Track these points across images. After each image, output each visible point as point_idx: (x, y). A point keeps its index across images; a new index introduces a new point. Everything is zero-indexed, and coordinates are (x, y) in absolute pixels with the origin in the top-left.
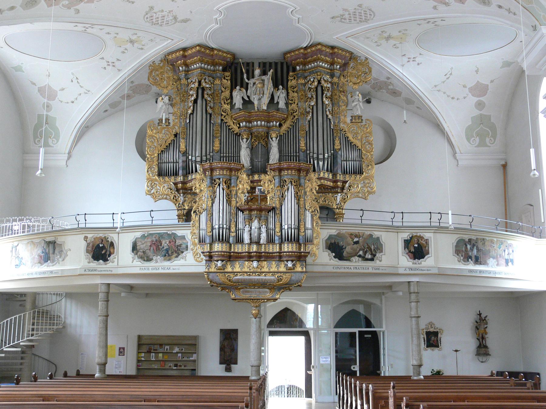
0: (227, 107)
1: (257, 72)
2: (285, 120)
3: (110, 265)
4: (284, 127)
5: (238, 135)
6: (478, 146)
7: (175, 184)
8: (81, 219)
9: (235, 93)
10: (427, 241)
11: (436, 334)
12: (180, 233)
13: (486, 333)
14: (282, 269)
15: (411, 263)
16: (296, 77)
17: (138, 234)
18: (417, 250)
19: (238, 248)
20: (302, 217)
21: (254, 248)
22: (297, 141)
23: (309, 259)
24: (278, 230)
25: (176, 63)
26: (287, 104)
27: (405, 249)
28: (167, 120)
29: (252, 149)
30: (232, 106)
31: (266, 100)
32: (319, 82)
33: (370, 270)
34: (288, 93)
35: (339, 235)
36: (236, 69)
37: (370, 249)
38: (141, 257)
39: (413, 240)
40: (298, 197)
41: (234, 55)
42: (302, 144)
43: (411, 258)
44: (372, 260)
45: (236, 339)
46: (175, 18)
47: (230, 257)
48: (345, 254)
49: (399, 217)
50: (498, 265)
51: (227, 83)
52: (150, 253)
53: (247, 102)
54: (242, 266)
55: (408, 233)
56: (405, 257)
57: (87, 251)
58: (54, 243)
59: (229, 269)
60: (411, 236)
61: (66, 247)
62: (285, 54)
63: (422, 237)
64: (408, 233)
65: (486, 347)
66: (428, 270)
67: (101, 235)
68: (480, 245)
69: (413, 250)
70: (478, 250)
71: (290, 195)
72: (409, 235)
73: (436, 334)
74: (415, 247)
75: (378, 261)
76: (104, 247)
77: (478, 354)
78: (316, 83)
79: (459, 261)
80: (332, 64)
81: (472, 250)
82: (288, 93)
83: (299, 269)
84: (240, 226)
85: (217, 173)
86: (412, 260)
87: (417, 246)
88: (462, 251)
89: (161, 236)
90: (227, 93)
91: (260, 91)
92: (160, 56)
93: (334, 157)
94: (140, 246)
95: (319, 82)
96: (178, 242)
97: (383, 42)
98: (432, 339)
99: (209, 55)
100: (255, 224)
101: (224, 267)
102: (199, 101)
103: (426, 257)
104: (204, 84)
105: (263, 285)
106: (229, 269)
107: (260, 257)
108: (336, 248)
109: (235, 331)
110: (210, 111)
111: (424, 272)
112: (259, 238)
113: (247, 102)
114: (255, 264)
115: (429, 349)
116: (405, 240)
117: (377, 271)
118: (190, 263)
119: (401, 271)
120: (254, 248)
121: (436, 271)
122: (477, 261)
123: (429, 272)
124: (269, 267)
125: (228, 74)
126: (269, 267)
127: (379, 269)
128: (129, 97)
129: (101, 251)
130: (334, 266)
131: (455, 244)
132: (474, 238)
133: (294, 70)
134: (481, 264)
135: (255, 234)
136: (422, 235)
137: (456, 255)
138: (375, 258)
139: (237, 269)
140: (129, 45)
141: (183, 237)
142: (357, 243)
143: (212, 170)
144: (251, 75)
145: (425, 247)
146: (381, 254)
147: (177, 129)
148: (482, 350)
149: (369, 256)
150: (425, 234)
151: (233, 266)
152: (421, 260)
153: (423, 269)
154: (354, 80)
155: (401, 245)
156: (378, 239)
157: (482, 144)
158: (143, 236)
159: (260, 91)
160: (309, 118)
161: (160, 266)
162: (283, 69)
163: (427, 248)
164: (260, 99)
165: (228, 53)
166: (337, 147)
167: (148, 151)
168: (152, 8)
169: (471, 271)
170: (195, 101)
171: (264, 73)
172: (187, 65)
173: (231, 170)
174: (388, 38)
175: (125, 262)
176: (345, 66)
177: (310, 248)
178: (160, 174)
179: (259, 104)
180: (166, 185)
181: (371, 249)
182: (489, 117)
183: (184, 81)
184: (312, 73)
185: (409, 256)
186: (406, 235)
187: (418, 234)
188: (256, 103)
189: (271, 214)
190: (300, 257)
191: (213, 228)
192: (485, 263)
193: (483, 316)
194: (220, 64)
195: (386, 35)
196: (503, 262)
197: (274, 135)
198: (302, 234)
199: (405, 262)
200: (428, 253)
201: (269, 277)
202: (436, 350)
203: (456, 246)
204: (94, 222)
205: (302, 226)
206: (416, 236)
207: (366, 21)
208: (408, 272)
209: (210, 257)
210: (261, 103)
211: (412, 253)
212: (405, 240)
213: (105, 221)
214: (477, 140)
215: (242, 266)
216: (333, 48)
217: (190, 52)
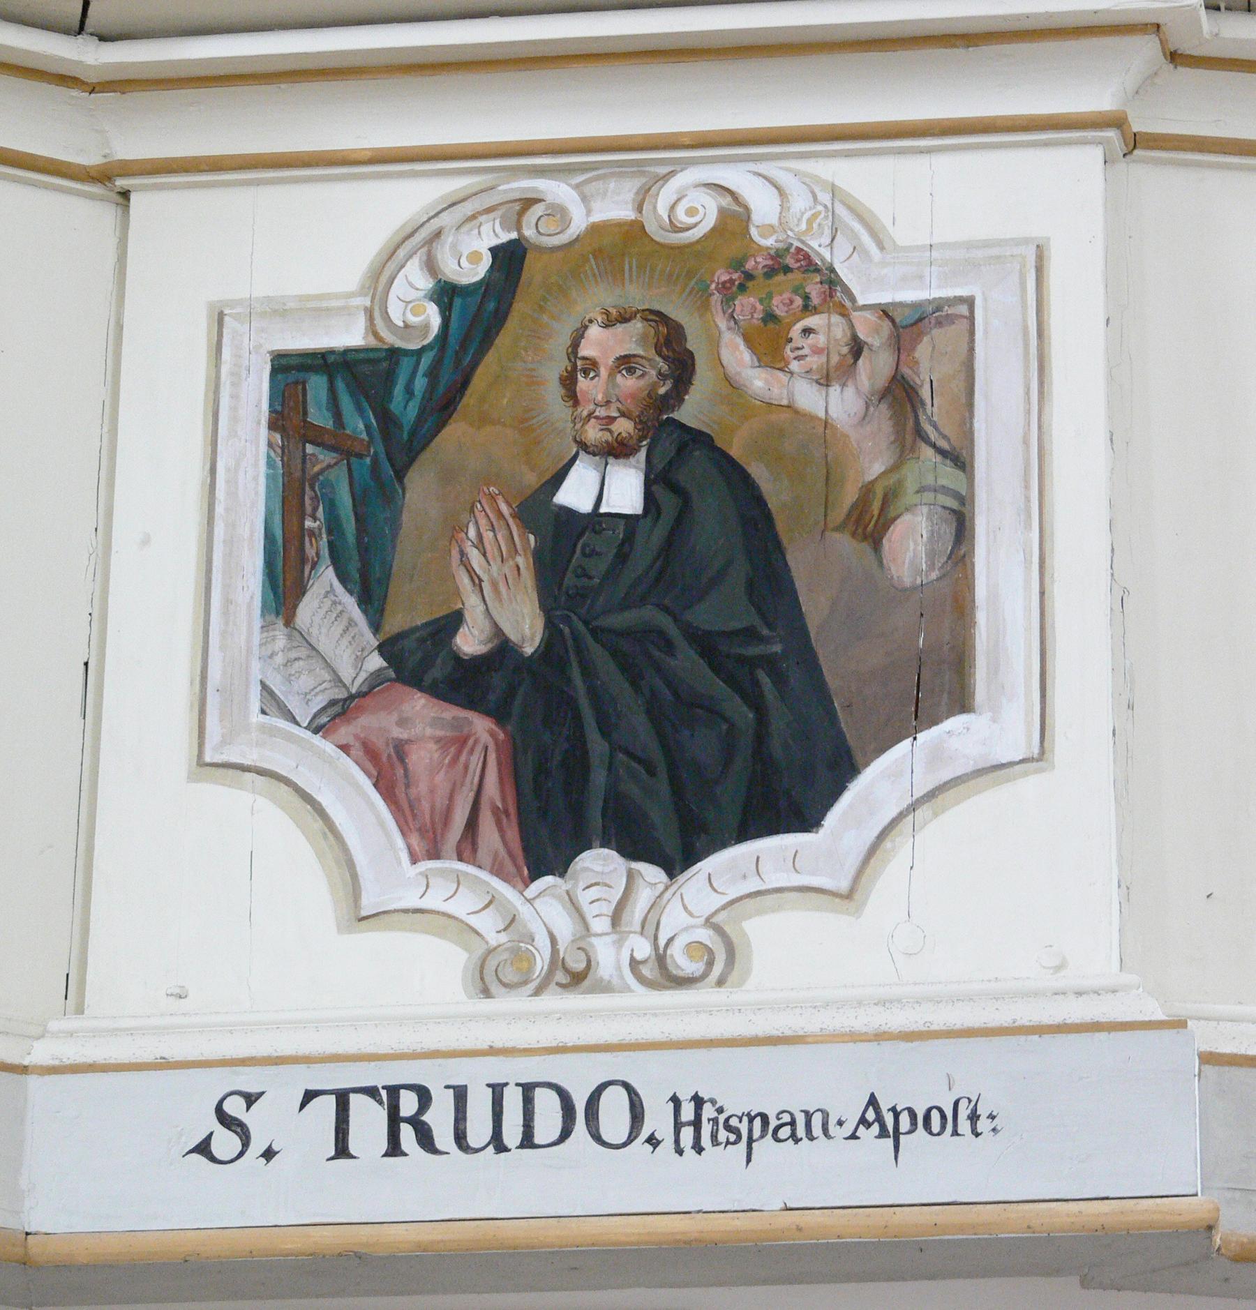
10: (916, 373)
27: (284, 590)
39: (524, 362)
60: (469, 260)
66: (884, 1122)
69: (502, 609)
72: (422, 238)
74: (564, 542)
86: (469, 893)
87: (625, 491)
116: (291, 371)
123: (935, 1175)
136: (775, 202)
145: (870, 522)
150: (862, 176)
152: (730, 867)
155: (189, 481)
185: (387, 771)
186: (337, 255)
187: (687, 203)
200: (938, 681)
206: (620, 247)
212: (291, 371)
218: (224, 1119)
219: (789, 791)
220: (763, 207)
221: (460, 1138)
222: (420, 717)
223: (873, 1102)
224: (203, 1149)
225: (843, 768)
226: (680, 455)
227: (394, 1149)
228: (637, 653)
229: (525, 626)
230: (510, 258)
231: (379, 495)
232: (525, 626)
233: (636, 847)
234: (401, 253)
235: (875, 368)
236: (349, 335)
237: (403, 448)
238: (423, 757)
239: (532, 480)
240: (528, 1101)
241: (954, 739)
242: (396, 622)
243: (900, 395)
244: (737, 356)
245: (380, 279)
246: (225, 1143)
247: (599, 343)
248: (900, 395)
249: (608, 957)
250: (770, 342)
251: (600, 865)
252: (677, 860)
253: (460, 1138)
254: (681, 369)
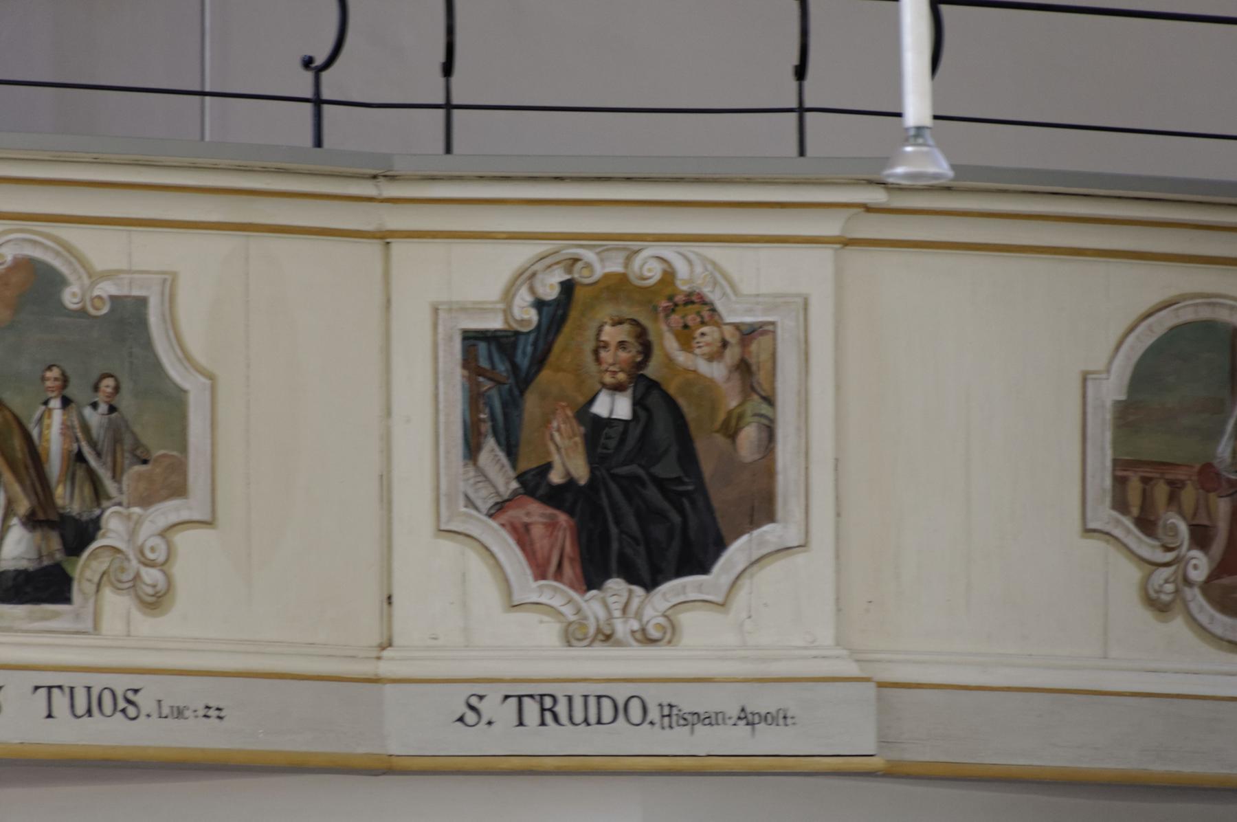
15: (547, 632)
27: (472, 450)
43: (540, 573)
55: (524, 253)
56: (476, 565)
60: (549, 288)
63: (695, 300)
64: (524, 253)
66: (747, 718)
69: (570, 463)
72: (527, 276)
74: (596, 428)
75: (115, 604)
79: (1158, 606)
86: (557, 595)
88: (1208, 476)
103: (737, 553)
111: (705, 741)
116: (471, 339)
117: (107, 733)
121: (852, 732)
123: (769, 740)
127: (127, 705)
131: (1113, 389)
136: (689, 270)
137: (1125, 528)
138: (86, 569)
145: (731, 430)
146: (167, 512)
153: (689, 700)
156: (127, 319)
163: (749, 435)
181: (36, 457)
185: (522, 535)
186: (487, 277)
199: (479, 612)
200: (761, 507)
203: (1128, 416)
206: (617, 287)
208: (501, 737)
211: (557, 497)
218: (472, 708)
219: (697, 555)
220: (682, 269)
221: (571, 718)
222: (535, 512)
223: (743, 710)
224: (461, 719)
225: (720, 545)
226: (646, 391)
227: (543, 723)
228: (630, 486)
229: (580, 470)
230: (568, 287)
231: (512, 404)
232: (580, 470)
233: (632, 577)
234: (518, 282)
235: (732, 354)
236: (495, 323)
237: (523, 381)
238: (538, 531)
239: (581, 400)
240: (599, 704)
241: (769, 534)
242: (524, 465)
243: (744, 368)
244: (671, 344)
245: (509, 295)
246: (471, 717)
247: (611, 334)
248: (744, 368)
249: (622, 628)
250: (686, 337)
251: (616, 586)
252: (650, 585)
253: (571, 718)
254: (646, 349)
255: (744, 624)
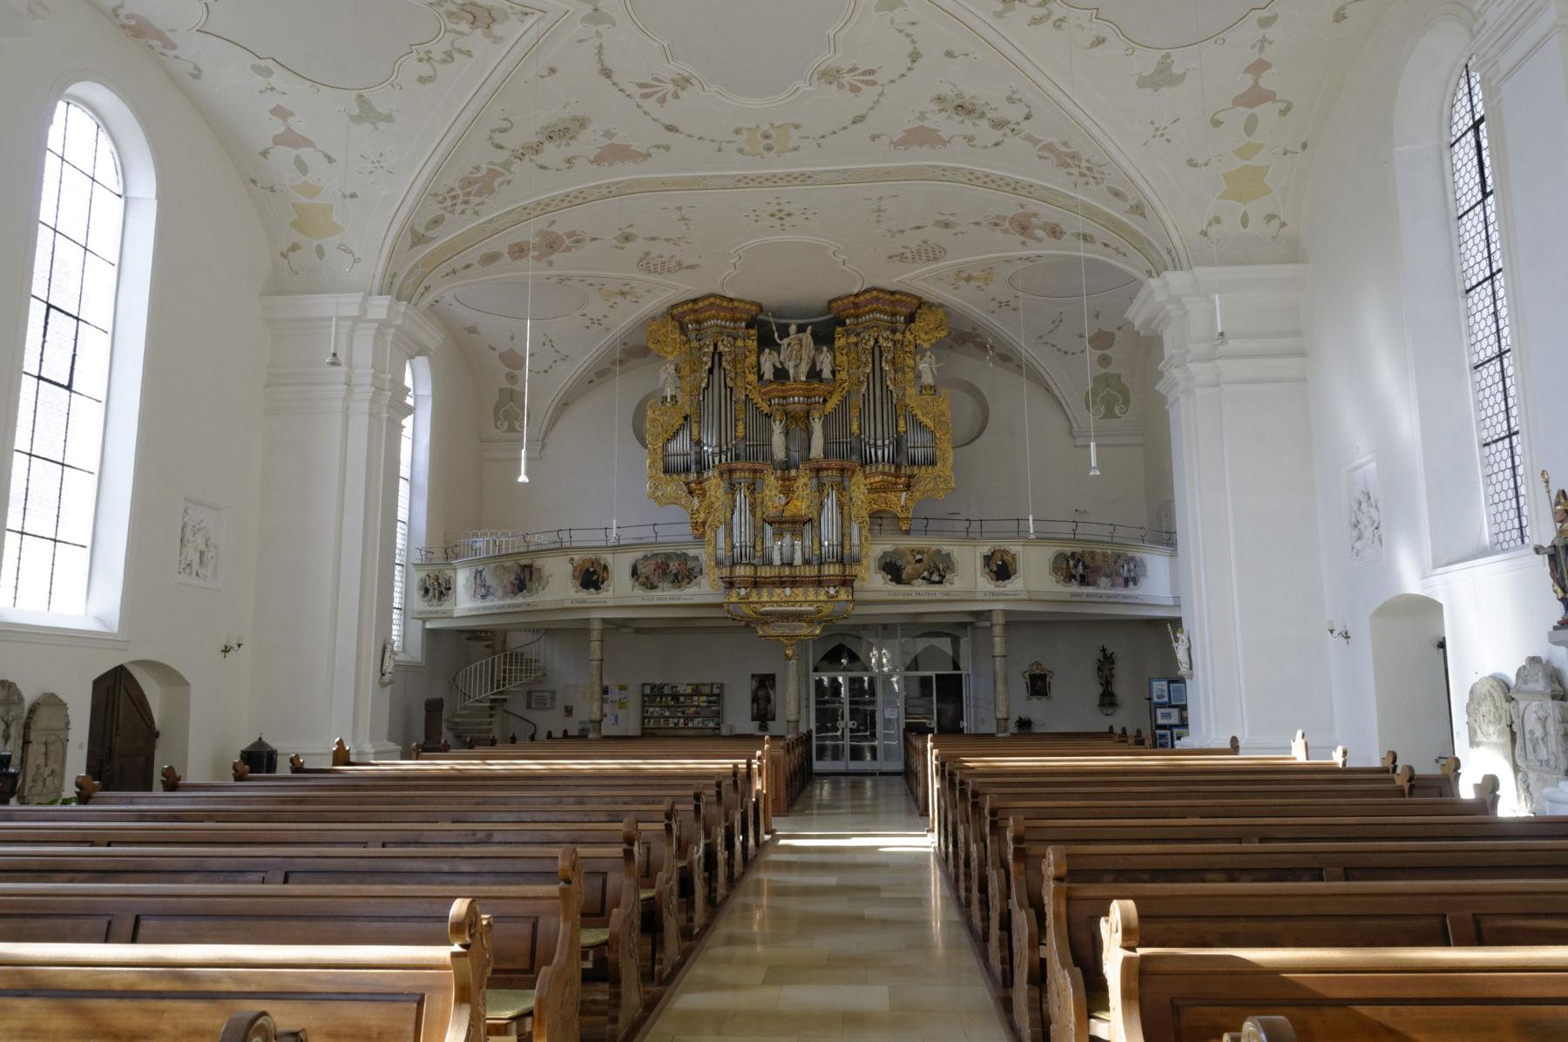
0: (752, 378)
1: (793, 329)
2: (831, 393)
3: (603, 594)
4: (830, 406)
5: (768, 416)
6: (1104, 417)
7: (687, 484)
8: (565, 535)
9: (762, 359)
10: (1014, 557)
11: (1043, 677)
12: (692, 552)
13: (1112, 676)
14: (823, 597)
16: (848, 334)
17: (639, 555)
18: (1002, 569)
19: (765, 572)
20: (846, 531)
21: (787, 571)
22: (846, 422)
23: (856, 584)
24: (816, 546)
25: (685, 318)
26: (833, 373)
28: (674, 397)
29: (787, 433)
30: (761, 377)
31: (804, 368)
32: (876, 341)
33: (938, 597)
34: (835, 358)
35: (896, 552)
36: (765, 328)
37: (938, 569)
38: (644, 584)
40: (841, 506)
41: (761, 309)
42: (855, 427)
44: (940, 582)
45: (773, 686)
46: (679, 264)
47: (756, 584)
48: (904, 576)
49: (975, 526)
50: (1113, 585)
51: (752, 344)
52: (654, 579)
53: (781, 374)
54: (771, 595)
57: (574, 577)
58: (530, 567)
59: (754, 598)
61: (546, 572)
62: (830, 302)
65: (1112, 695)
67: (591, 555)
68: (1087, 559)
70: (1085, 567)
71: (831, 503)
73: (1043, 677)
76: (595, 572)
77: (1102, 704)
78: (872, 342)
80: (894, 315)
81: (1076, 566)
82: (835, 358)
83: (843, 596)
84: (768, 543)
85: (737, 475)
89: (668, 556)
90: (752, 359)
91: (797, 354)
92: (664, 308)
93: (898, 443)
94: (642, 570)
95: (876, 341)
96: (690, 564)
97: (962, 283)
98: (1038, 685)
99: (726, 309)
100: (787, 539)
101: (748, 596)
102: (716, 371)
104: (721, 348)
105: (798, 616)
106: (754, 598)
107: (794, 582)
108: (892, 569)
109: (772, 677)
110: (730, 384)
112: (793, 559)
113: (781, 374)
114: (788, 591)
115: (1034, 700)
118: (704, 590)
119: (978, 597)
120: (787, 571)
121: (1026, 596)
122: (1084, 581)
124: (806, 594)
125: (752, 332)
126: (806, 594)
128: (621, 362)
129: (591, 578)
130: (889, 592)
132: (1078, 550)
133: (843, 324)
134: (1088, 584)
135: (787, 553)
139: (765, 598)
140: (619, 299)
141: (696, 558)
142: (920, 561)
143: (731, 471)
144: (784, 332)
147: (688, 410)
148: (1108, 700)
149: (936, 578)
151: (759, 595)
154: (925, 337)
155: (979, 562)
157: (1110, 414)
158: (646, 558)
159: (797, 354)
160: (863, 390)
161: (667, 594)
162: (827, 326)
164: (796, 366)
165: (752, 303)
166: (902, 428)
167: (649, 439)
168: (647, 254)
169: (1073, 595)
170: (711, 371)
171: (801, 329)
172: (698, 322)
173: (755, 471)
174: (969, 279)
175: (621, 592)
176: (911, 319)
177: (856, 569)
178: (665, 472)
179: (796, 372)
180: (675, 486)
182: (1119, 376)
183: (695, 344)
184: (867, 328)
186: (986, 549)
188: (791, 372)
189: (808, 527)
190: (846, 582)
191: (733, 547)
192: (1095, 584)
193: (1108, 652)
194: (741, 320)
195: (964, 275)
196: (1121, 581)
197: (816, 415)
198: (847, 552)
199: (985, 584)
201: (806, 608)
202: (1044, 699)
204: (580, 539)
205: (847, 543)
207: (936, 259)
209: (730, 584)
210: (799, 372)
213: (597, 539)
214: (1103, 409)
215: (771, 595)
216: (893, 293)
217: (701, 305)
255: (1015, 585)
